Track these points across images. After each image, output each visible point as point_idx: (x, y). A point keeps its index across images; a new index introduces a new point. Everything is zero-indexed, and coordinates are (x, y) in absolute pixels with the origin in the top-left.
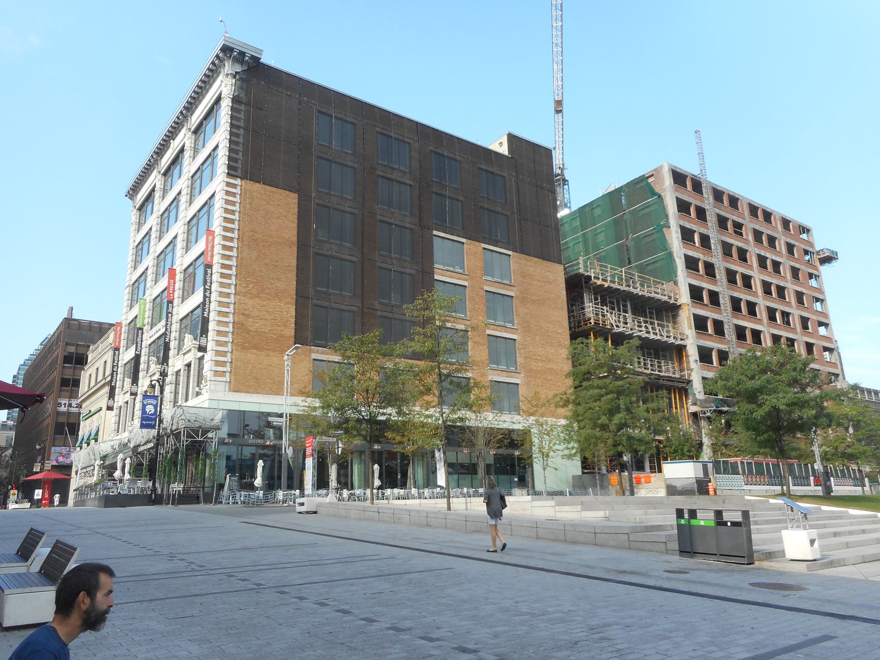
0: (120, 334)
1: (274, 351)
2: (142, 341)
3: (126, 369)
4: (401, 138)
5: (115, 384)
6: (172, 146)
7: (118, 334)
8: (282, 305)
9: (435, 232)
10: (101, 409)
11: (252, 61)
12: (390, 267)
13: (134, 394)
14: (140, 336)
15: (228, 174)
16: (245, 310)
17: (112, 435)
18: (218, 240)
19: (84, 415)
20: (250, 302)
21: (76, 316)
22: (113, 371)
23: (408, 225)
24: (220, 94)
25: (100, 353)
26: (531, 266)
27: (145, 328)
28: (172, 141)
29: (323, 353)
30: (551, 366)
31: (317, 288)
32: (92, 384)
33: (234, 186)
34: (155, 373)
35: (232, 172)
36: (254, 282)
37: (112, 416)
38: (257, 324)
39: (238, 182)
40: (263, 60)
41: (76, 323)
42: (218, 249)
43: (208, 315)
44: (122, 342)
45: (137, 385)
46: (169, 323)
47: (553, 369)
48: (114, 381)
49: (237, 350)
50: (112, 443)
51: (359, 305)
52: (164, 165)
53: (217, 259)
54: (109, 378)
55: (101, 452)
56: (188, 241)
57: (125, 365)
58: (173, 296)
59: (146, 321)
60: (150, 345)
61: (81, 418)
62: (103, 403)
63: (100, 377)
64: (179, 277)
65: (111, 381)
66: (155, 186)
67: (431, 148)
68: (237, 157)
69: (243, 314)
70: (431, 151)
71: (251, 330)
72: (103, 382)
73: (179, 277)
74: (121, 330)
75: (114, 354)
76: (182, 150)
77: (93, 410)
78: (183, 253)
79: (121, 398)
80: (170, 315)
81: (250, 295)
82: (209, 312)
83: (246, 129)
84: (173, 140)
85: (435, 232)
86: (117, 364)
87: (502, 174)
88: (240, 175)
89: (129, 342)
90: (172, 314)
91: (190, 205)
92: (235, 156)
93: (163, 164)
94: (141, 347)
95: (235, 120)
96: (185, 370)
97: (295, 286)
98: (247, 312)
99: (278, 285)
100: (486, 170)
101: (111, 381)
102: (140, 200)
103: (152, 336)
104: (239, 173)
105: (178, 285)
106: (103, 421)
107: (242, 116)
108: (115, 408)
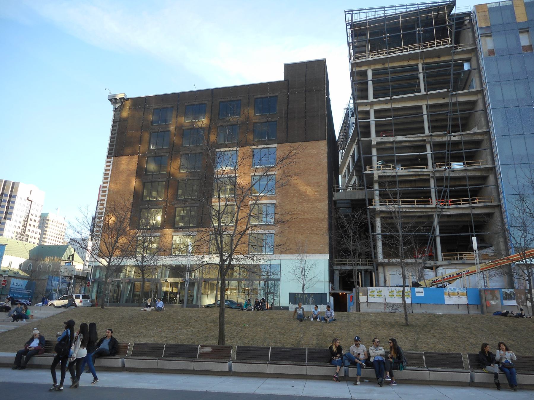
4: (200, 103)
15: (108, 157)
30: (306, 216)
47: (308, 219)
67: (220, 100)
87: (274, 95)
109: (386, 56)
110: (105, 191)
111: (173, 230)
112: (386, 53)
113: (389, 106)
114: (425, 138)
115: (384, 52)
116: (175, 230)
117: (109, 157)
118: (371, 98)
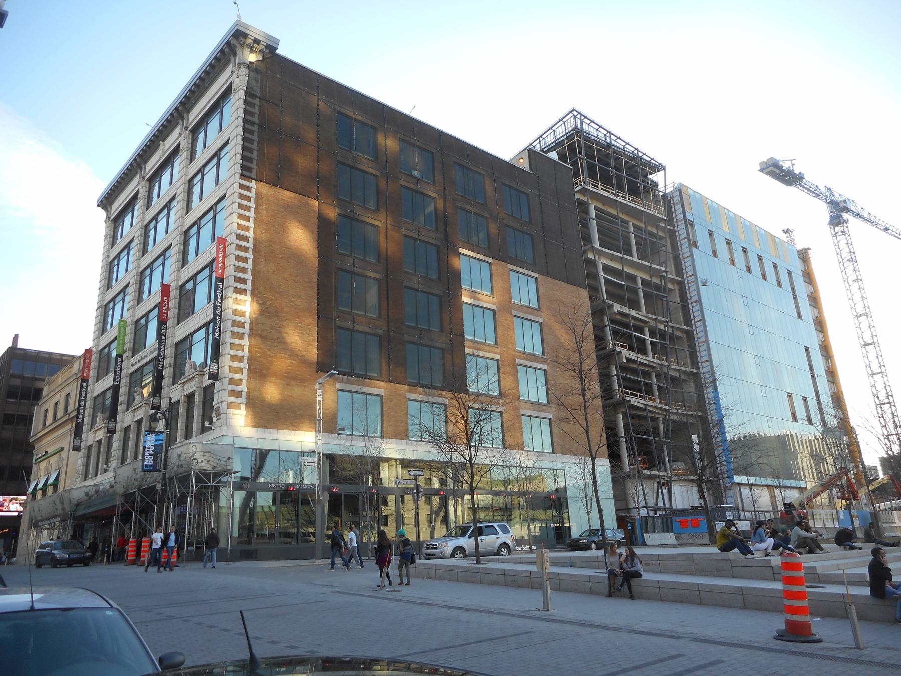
0: (90, 363)
2: (121, 370)
3: (97, 403)
5: (82, 420)
6: (161, 147)
7: (86, 363)
8: (303, 326)
9: (461, 250)
10: (62, 449)
11: (268, 51)
12: (416, 286)
13: (112, 431)
14: (119, 364)
15: (242, 175)
16: (263, 331)
17: (79, 480)
18: (232, 250)
19: (38, 456)
21: (21, 345)
22: (79, 406)
23: (432, 241)
24: (230, 85)
25: (61, 384)
27: (124, 355)
28: (161, 142)
29: (349, 382)
31: (340, 308)
32: (49, 420)
33: (248, 189)
34: (141, 405)
35: (246, 173)
36: (272, 300)
37: (78, 459)
38: (276, 348)
39: (253, 184)
41: (22, 352)
42: (231, 261)
43: (219, 336)
44: (91, 372)
45: (115, 421)
46: (163, 347)
48: (81, 417)
49: (253, 378)
50: (86, 490)
51: (385, 329)
52: (150, 170)
53: (230, 272)
54: (75, 413)
55: (72, 500)
56: (185, 253)
57: (95, 398)
58: (167, 315)
59: (126, 346)
60: (131, 374)
61: (34, 460)
62: (66, 442)
63: (60, 413)
64: (174, 294)
65: (77, 416)
66: (137, 193)
68: (252, 156)
70: (455, 162)
71: (269, 355)
72: (66, 417)
73: (174, 294)
74: (90, 358)
75: (81, 385)
76: (176, 151)
77: (51, 450)
78: (178, 267)
79: (90, 437)
80: (163, 338)
81: (267, 315)
82: (220, 333)
83: (261, 126)
84: (163, 141)
85: (461, 250)
86: (85, 397)
88: (255, 177)
89: (101, 372)
90: (165, 336)
91: (187, 213)
92: (248, 154)
93: (147, 169)
94: (120, 376)
95: (249, 115)
96: (185, 402)
97: (316, 305)
98: (264, 334)
100: (510, 187)
101: (77, 416)
102: (116, 210)
103: (135, 363)
104: (254, 175)
105: (173, 303)
106: (65, 463)
107: (256, 110)
108: (82, 447)
109: (615, 198)
111: (407, 387)
112: (613, 194)
113: (618, 266)
114: (650, 321)
115: (611, 191)
116: (411, 387)
117: (246, 176)
118: (597, 245)
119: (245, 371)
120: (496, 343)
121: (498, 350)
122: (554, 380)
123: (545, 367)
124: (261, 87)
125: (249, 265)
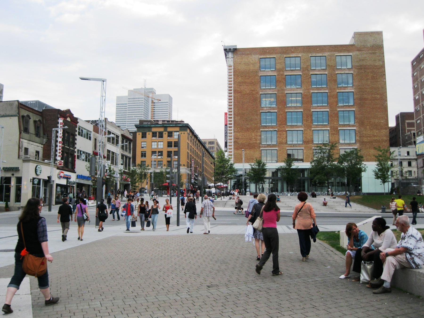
1: (247, 149)
20: (239, 134)
26: (365, 94)
30: (375, 138)
40: (238, 47)
47: (377, 140)
69: (236, 138)
98: (237, 138)
99: (248, 126)
110: (231, 118)
119: (233, 149)
120: (329, 124)
121: (329, 126)
122: (359, 133)
123: (355, 128)
124: (234, 62)
125: (233, 119)
